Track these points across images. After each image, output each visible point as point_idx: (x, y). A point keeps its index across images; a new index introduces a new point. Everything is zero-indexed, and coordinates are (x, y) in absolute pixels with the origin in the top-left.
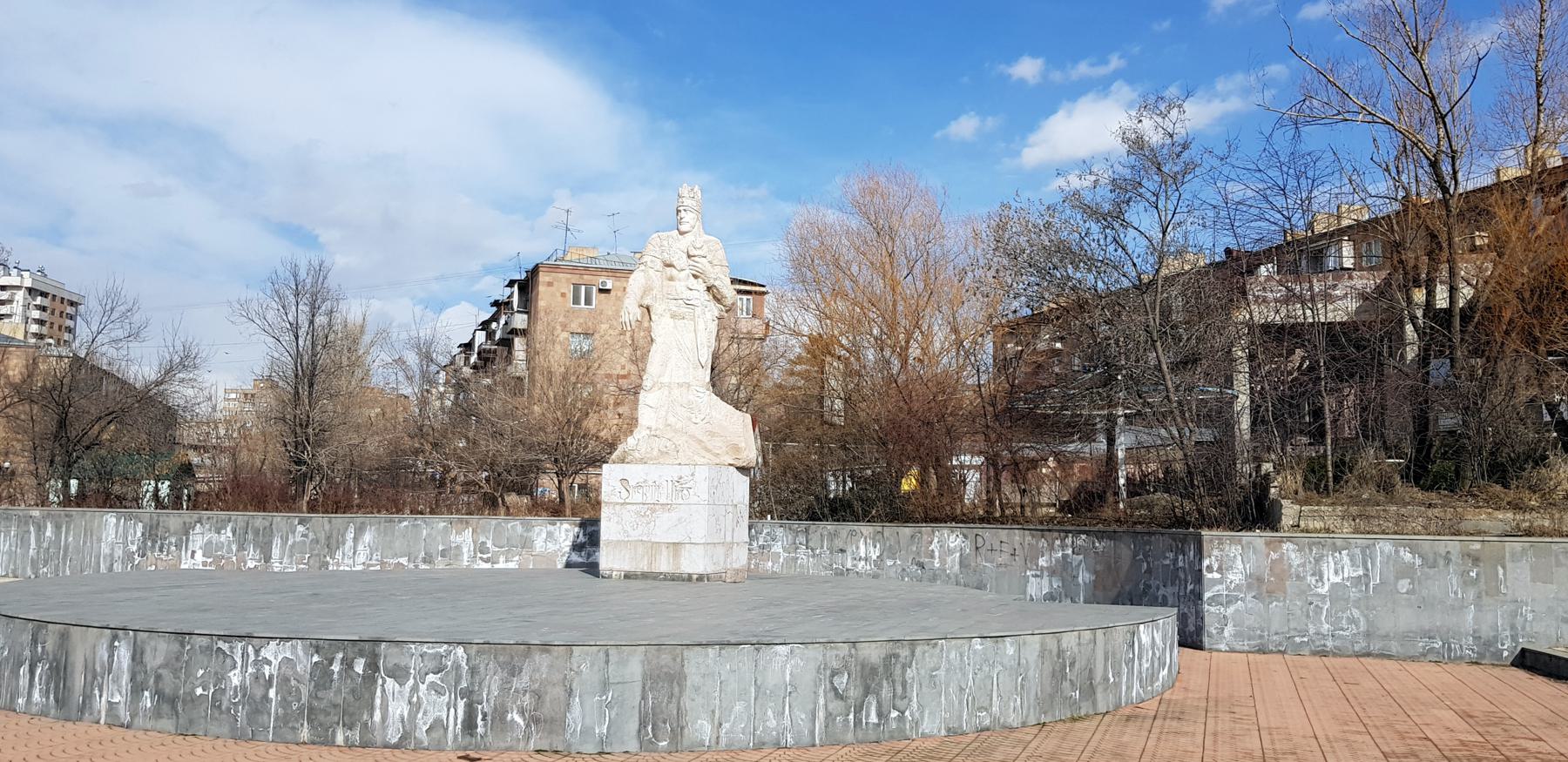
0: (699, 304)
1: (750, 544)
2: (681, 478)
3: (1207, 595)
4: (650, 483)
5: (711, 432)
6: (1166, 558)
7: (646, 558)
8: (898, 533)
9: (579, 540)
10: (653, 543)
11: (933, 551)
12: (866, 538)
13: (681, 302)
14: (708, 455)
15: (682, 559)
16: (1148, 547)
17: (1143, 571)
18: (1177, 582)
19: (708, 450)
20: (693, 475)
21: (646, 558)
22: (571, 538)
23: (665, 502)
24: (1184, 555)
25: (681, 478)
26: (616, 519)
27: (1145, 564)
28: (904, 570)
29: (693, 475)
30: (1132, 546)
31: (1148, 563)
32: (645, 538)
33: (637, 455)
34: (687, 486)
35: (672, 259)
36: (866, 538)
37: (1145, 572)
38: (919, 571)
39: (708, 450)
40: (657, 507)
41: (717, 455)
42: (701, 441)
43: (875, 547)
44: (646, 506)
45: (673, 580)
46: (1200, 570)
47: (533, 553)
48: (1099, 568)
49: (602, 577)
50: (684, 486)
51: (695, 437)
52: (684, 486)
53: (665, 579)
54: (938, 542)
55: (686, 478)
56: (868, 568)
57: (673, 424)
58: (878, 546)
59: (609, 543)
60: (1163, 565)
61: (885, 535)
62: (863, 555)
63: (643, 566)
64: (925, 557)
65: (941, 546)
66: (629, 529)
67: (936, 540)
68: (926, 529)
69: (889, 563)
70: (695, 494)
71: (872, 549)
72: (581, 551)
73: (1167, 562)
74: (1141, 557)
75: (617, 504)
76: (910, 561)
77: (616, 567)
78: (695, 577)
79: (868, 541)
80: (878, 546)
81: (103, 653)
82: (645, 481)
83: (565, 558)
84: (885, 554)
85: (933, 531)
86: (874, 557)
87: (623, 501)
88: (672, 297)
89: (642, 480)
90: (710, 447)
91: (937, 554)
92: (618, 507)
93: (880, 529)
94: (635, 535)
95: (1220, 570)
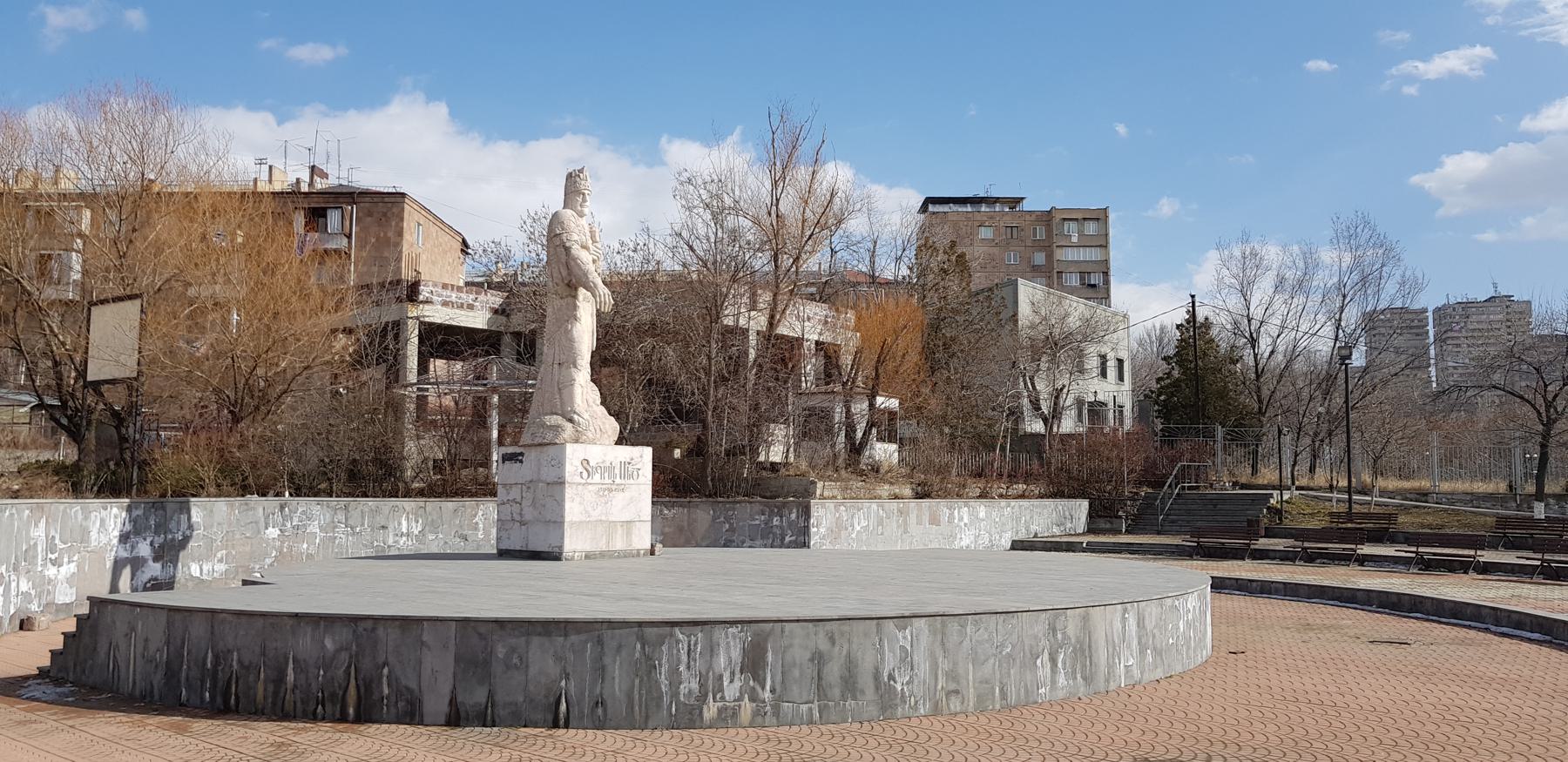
1: (284, 525)
2: (632, 459)
3: (812, 543)
6: (754, 520)
7: (604, 537)
8: (440, 508)
9: (125, 529)
10: (610, 522)
11: (477, 523)
12: (408, 513)
15: (633, 536)
16: (731, 513)
17: (724, 530)
18: (771, 535)
20: (641, 457)
21: (604, 537)
22: (119, 526)
24: (781, 517)
25: (632, 459)
26: (578, 499)
27: (727, 526)
28: (446, 543)
29: (641, 457)
30: (711, 512)
31: (731, 525)
32: (603, 518)
36: (408, 513)
37: (727, 531)
38: (462, 544)
40: (614, 487)
43: (418, 522)
44: (604, 486)
45: (625, 557)
46: (808, 526)
47: (89, 549)
48: (667, 530)
49: (566, 559)
53: (618, 557)
54: (483, 515)
56: (410, 543)
58: (420, 521)
59: (572, 523)
60: (750, 525)
61: (427, 509)
62: (404, 530)
63: (602, 546)
64: (468, 530)
65: (485, 519)
66: (590, 509)
67: (480, 513)
68: (469, 503)
69: (431, 537)
71: (414, 524)
72: (125, 543)
73: (757, 522)
74: (722, 519)
75: (580, 484)
76: (453, 534)
77: (579, 548)
78: (642, 552)
79: (411, 516)
80: (420, 521)
81: (1118, 625)
83: (113, 553)
84: (427, 528)
85: (477, 505)
86: (416, 532)
87: (584, 481)
91: (481, 526)
92: (580, 487)
93: (422, 504)
94: (595, 515)
95: (817, 527)
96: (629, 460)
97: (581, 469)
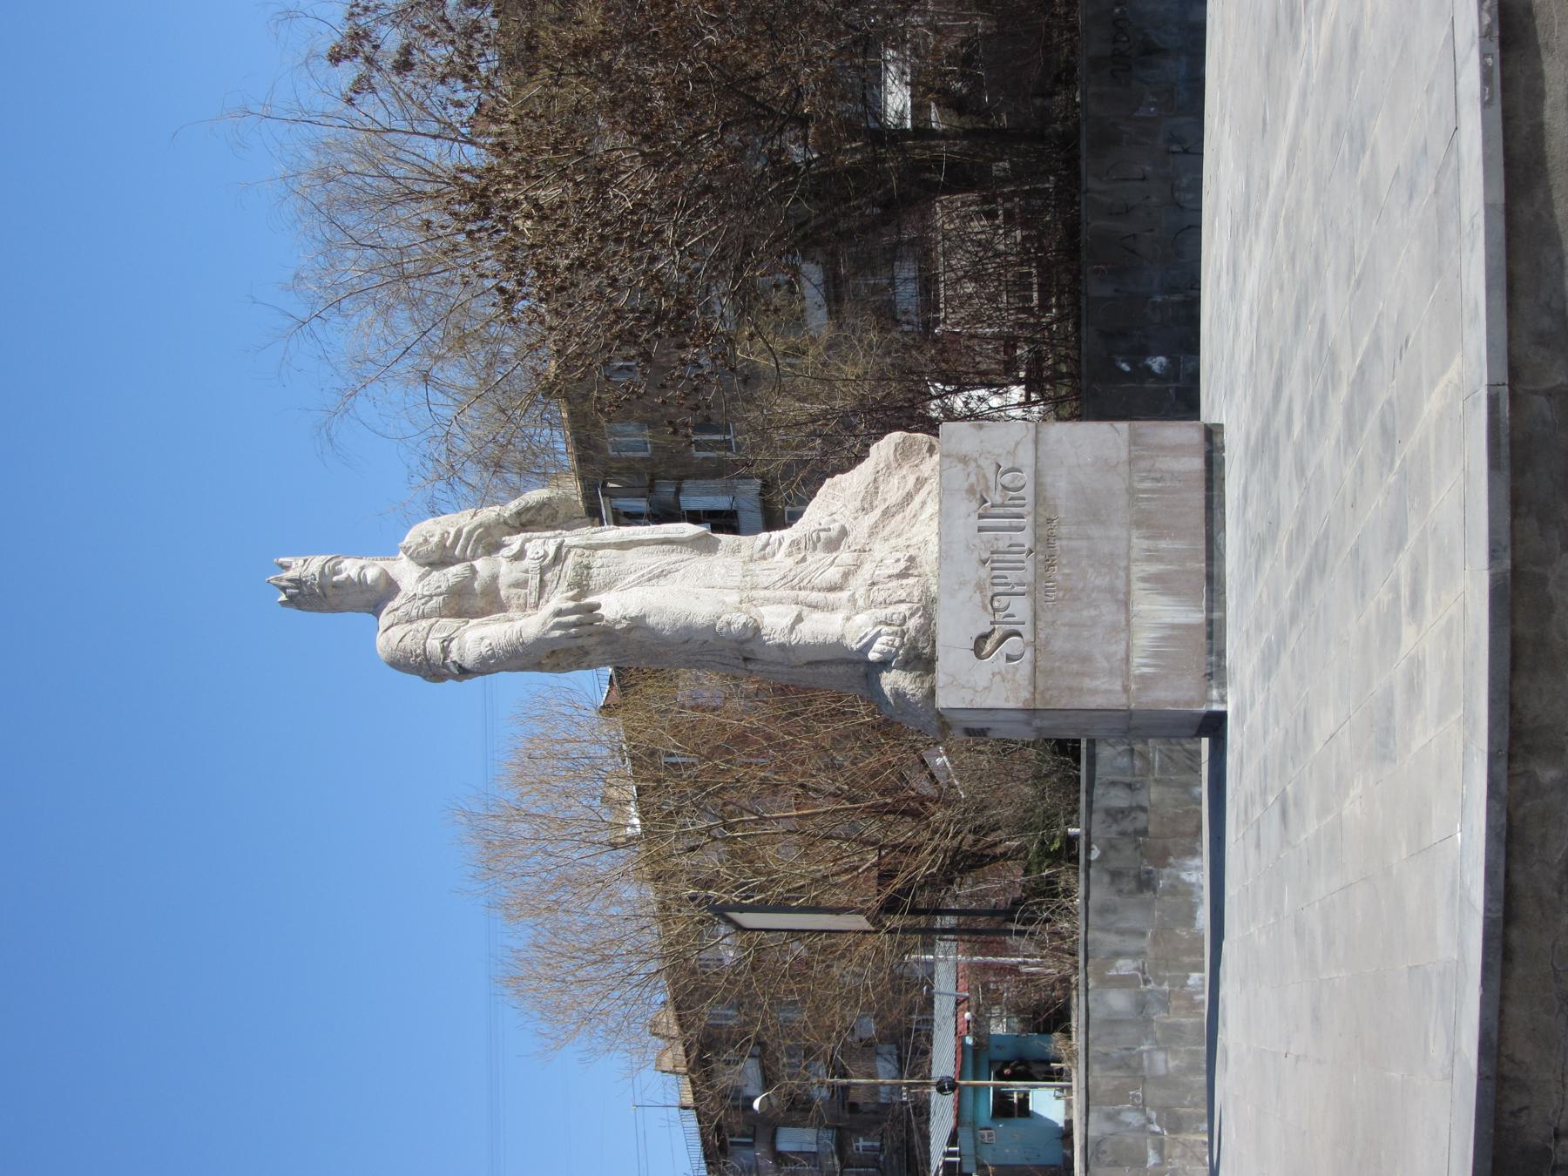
0: (559, 540)
2: (971, 491)
4: (984, 572)
5: (864, 499)
13: (548, 576)
14: (918, 499)
19: (909, 498)
23: (1028, 531)
33: (913, 623)
34: (992, 477)
35: (443, 588)
39: (909, 498)
41: (920, 483)
42: (885, 513)
50: (992, 484)
51: (876, 526)
52: (992, 484)
55: (973, 479)
57: (841, 569)
70: (1012, 453)
82: (980, 587)
88: (535, 594)
89: (977, 597)
90: (902, 493)
96: (974, 505)
97: (996, 661)
